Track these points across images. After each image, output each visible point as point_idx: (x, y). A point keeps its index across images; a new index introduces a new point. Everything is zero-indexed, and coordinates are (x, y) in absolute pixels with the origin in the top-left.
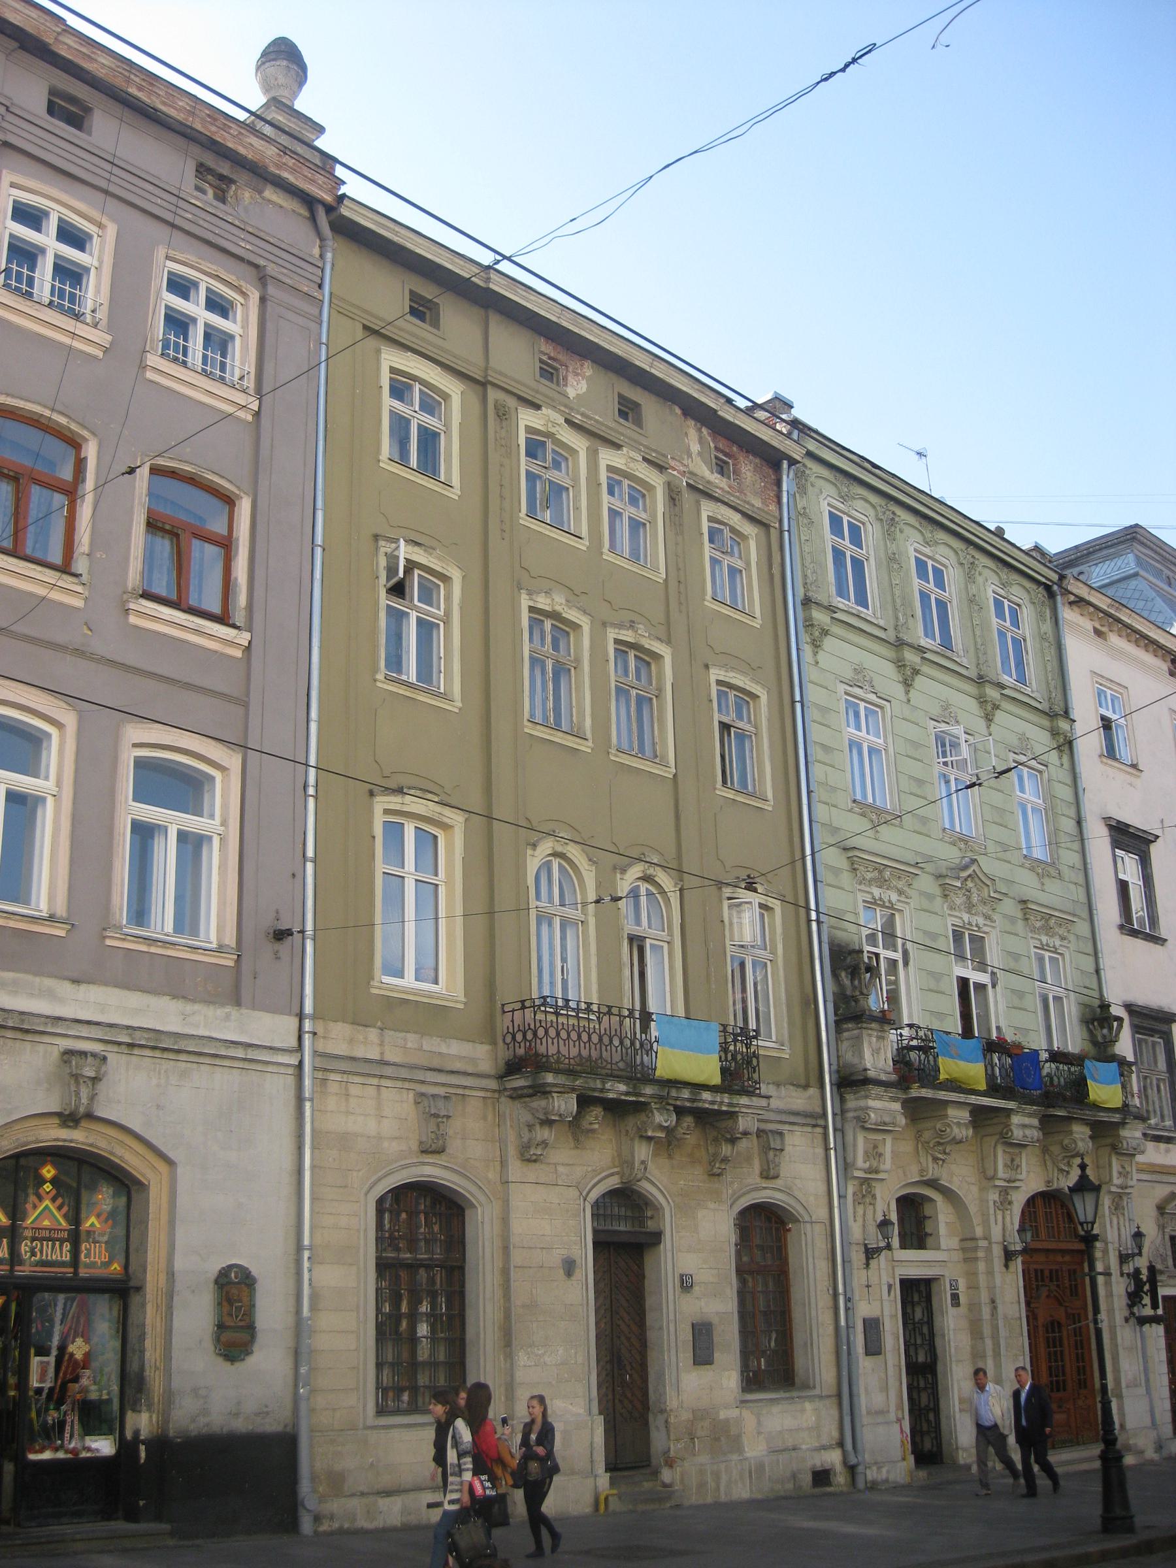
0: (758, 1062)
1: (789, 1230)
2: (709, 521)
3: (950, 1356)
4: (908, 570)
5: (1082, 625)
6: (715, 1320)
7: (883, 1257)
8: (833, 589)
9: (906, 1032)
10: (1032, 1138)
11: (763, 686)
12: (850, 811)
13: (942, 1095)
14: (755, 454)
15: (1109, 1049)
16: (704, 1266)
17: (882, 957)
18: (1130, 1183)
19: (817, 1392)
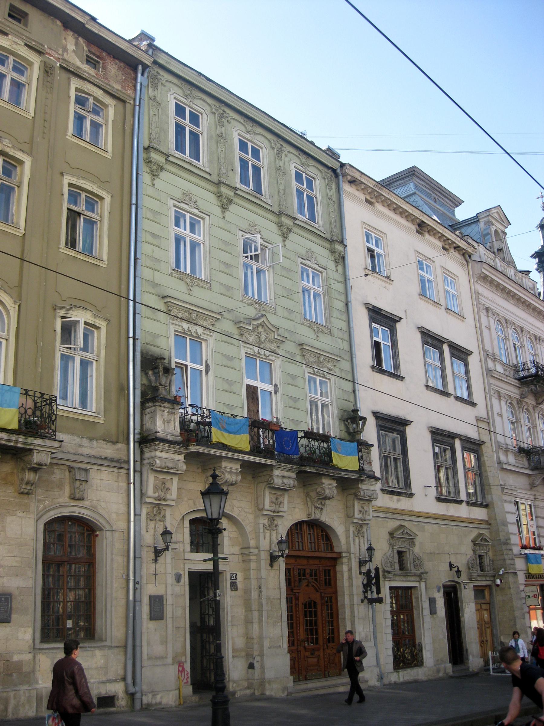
0: (56, 418)
1: (97, 536)
2: (76, 91)
3: (227, 622)
4: (232, 146)
5: (358, 196)
6: (16, 592)
7: (168, 555)
8: (173, 145)
9: (190, 410)
10: (289, 485)
11: (108, 192)
12: (171, 275)
13: (213, 452)
14: (120, 60)
15: (357, 436)
16: (9, 555)
17: (189, 367)
18: (367, 518)
19: (108, 643)
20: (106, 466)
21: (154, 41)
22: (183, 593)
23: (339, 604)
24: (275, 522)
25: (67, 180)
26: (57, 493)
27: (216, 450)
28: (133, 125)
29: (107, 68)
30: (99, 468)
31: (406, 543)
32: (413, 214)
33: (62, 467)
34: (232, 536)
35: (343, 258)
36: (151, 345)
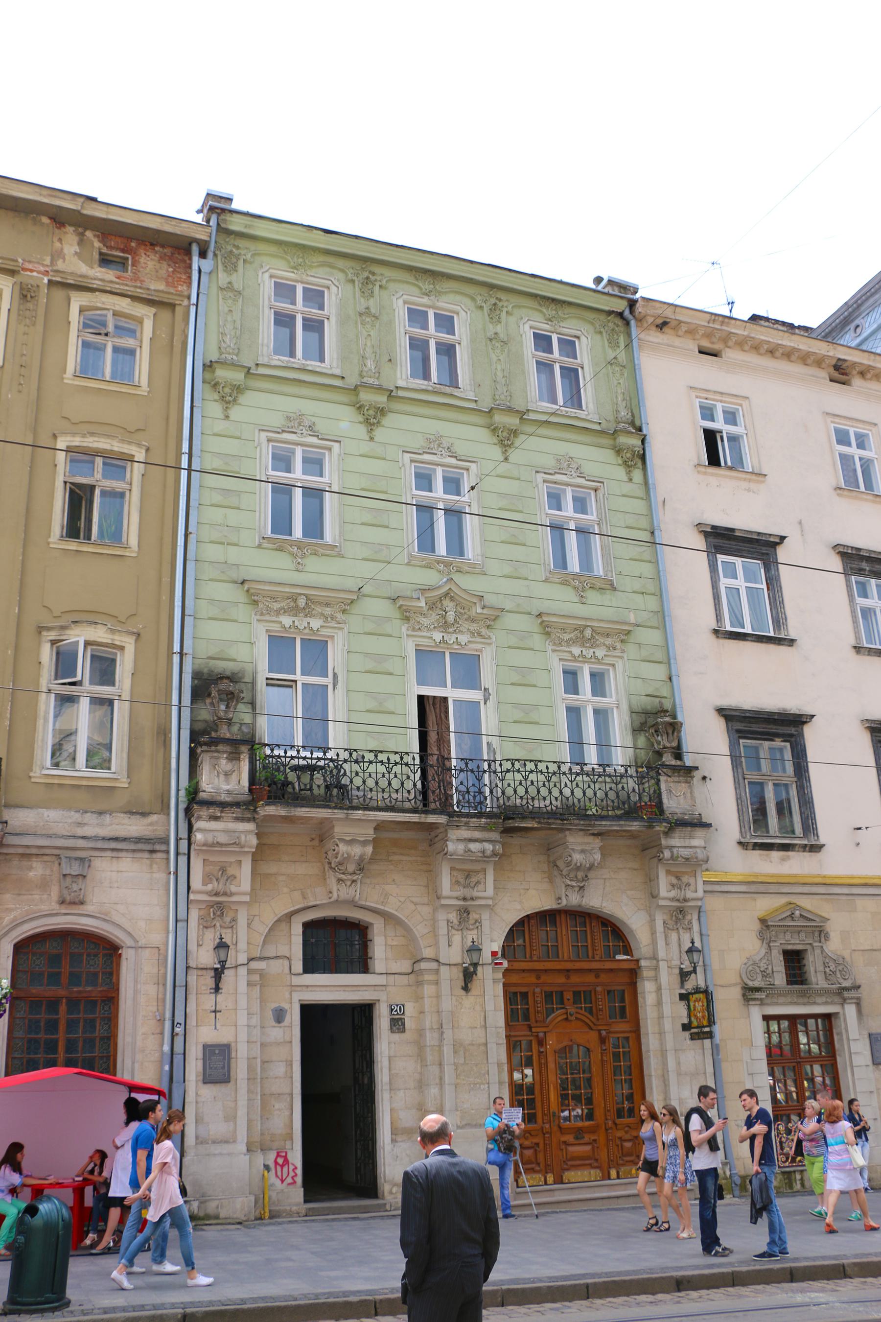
10: (484, 852)
12: (259, 546)
18: (690, 894)
20: (127, 850)
21: (230, 200)
22: (288, 1039)
23: (644, 1049)
24: (473, 916)
25: (61, 444)
26: (37, 897)
27: (307, 809)
28: (186, 337)
29: (139, 262)
30: (115, 854)
31: (803, 935)
32: (810, 350)
33: (46, 858)
34: (395, 943)
35: (643, 457)
36: (219, 659)
